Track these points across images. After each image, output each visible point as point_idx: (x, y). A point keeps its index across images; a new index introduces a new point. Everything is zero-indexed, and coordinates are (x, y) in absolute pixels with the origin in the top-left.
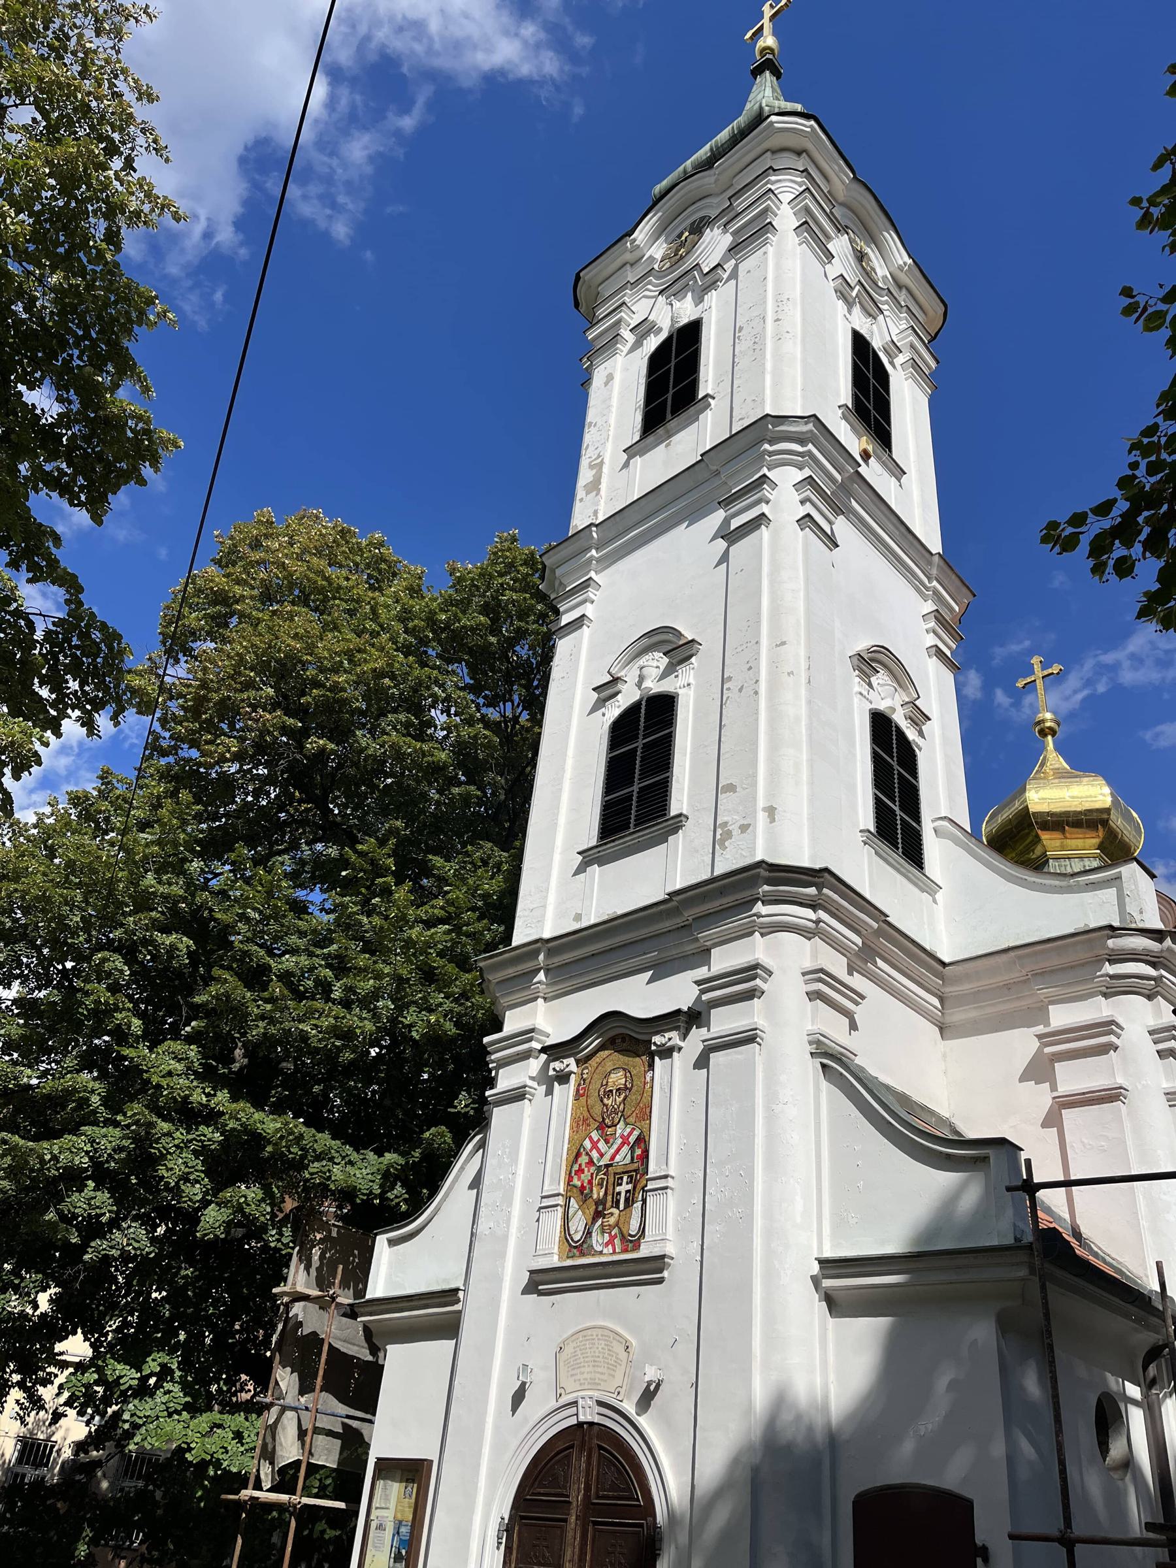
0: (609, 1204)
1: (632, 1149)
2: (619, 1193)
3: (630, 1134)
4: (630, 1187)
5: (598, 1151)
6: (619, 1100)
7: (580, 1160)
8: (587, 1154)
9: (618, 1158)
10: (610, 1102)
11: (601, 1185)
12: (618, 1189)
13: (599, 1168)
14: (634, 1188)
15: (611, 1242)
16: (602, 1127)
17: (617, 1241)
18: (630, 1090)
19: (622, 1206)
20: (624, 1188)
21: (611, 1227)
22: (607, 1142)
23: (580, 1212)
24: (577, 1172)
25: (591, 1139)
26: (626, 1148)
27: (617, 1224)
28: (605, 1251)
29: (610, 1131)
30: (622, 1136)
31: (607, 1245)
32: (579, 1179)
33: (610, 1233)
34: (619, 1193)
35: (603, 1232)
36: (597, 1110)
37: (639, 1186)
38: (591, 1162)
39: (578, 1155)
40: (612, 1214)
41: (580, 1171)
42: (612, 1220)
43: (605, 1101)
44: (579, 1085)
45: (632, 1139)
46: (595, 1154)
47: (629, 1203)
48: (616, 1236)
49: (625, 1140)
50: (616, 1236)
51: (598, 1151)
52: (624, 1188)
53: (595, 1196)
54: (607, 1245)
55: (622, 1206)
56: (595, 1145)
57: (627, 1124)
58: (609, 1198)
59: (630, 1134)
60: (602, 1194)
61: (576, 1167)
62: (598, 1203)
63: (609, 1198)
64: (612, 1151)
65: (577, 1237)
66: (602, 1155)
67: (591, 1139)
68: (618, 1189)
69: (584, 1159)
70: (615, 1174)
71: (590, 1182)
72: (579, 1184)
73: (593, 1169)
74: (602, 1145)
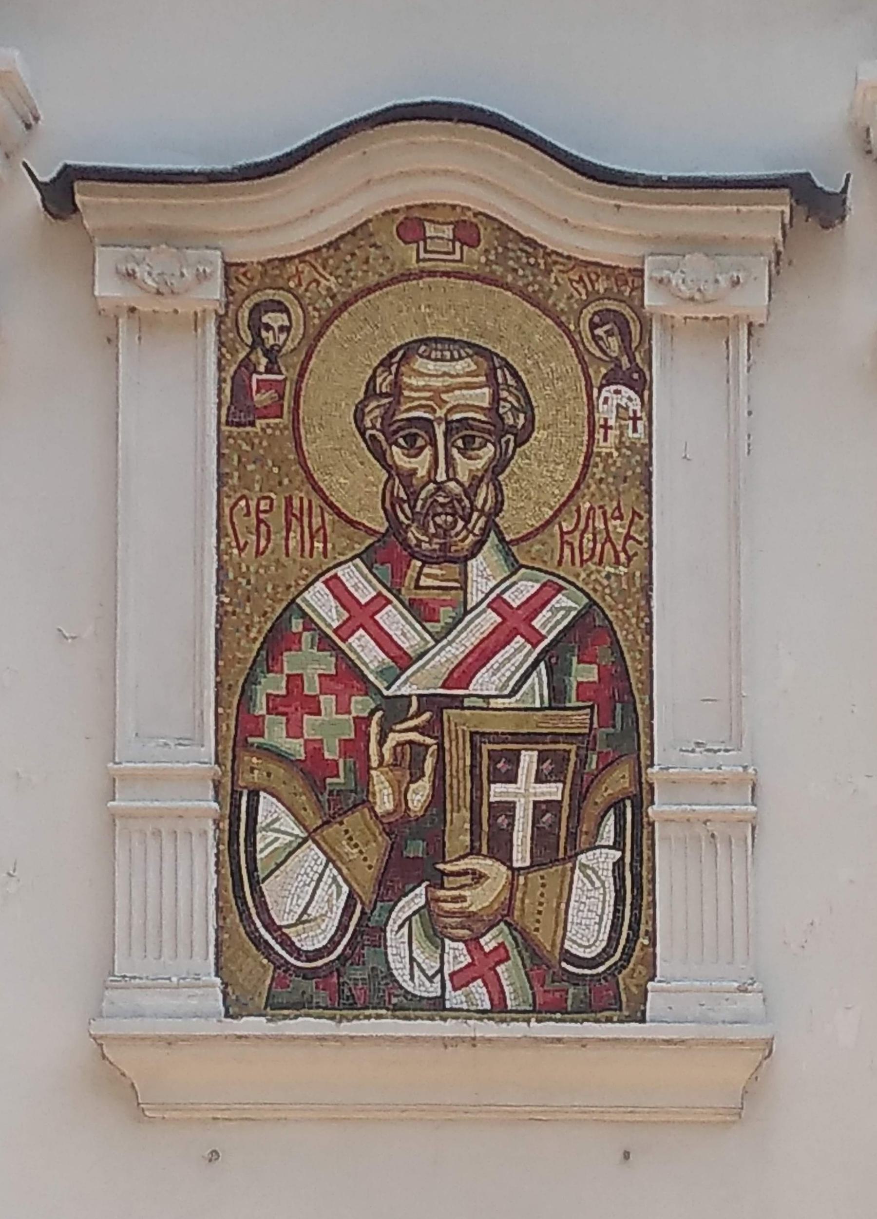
0: (458, 836)
1: (554, 658)
2: (509, 808)
3: (536, 604)
4: (553, 791)
5: (383, 640)
6: (465, 468)
7: (290, 662)
8: (324, 642)
9: (484, 682)
10: (421, 464)
11: (409, 762)
12: (498, 792)
13: (394, 710)
14: (580, 795)
15: (482, 968)
16: (388, 552)
17: (509, 974)
18: (523, 437)
19: (521, 857)
20: (526, 790)
21: (473, 925)
22: (421, 611)
23: (312, 855)
24: (275, 705)
25: (337, 588)
26: (517, 654)
27: (504, 913)
28: (455, 998)
29: (433, 576)
30: (498, 605)
31: (461, 979)
32: (295, 731)
33: (473, 943)
34: (509, 808)
35: (436, 936)
36: (356, 485)
37: (602, 794)
38: (349, 676)
39: (277, 642)
40: (478, 877)
41: (295, 702)
42: (479, 899)
43: (398, 455)
44: (247, 365)
45: (550, 622)
46: (365, 650)
47: (557, 845)
48: (501, 955)
49: (514, 623)
50: (501, 955)
51: (383, 640)
52: (526, 790)
53: (385, 802)
54: (461, 979)
55: (521, 857)
56: (360, 616)
57: (515, 567)
58: (459, 820)
59: (536, 604)
60: (419, 796)
61: (273, 685)
62: (397, 828)
63: (459, 820)
64: (455, 649)
65: (312, 939)
66: (402, 661)
67: (337, 588)
68: (498, 792)
69: (310, 664)
70: (476, 738)
71: (355, 748)
72: (296, 748)
73: (360, 705)
74: (394, 620)
